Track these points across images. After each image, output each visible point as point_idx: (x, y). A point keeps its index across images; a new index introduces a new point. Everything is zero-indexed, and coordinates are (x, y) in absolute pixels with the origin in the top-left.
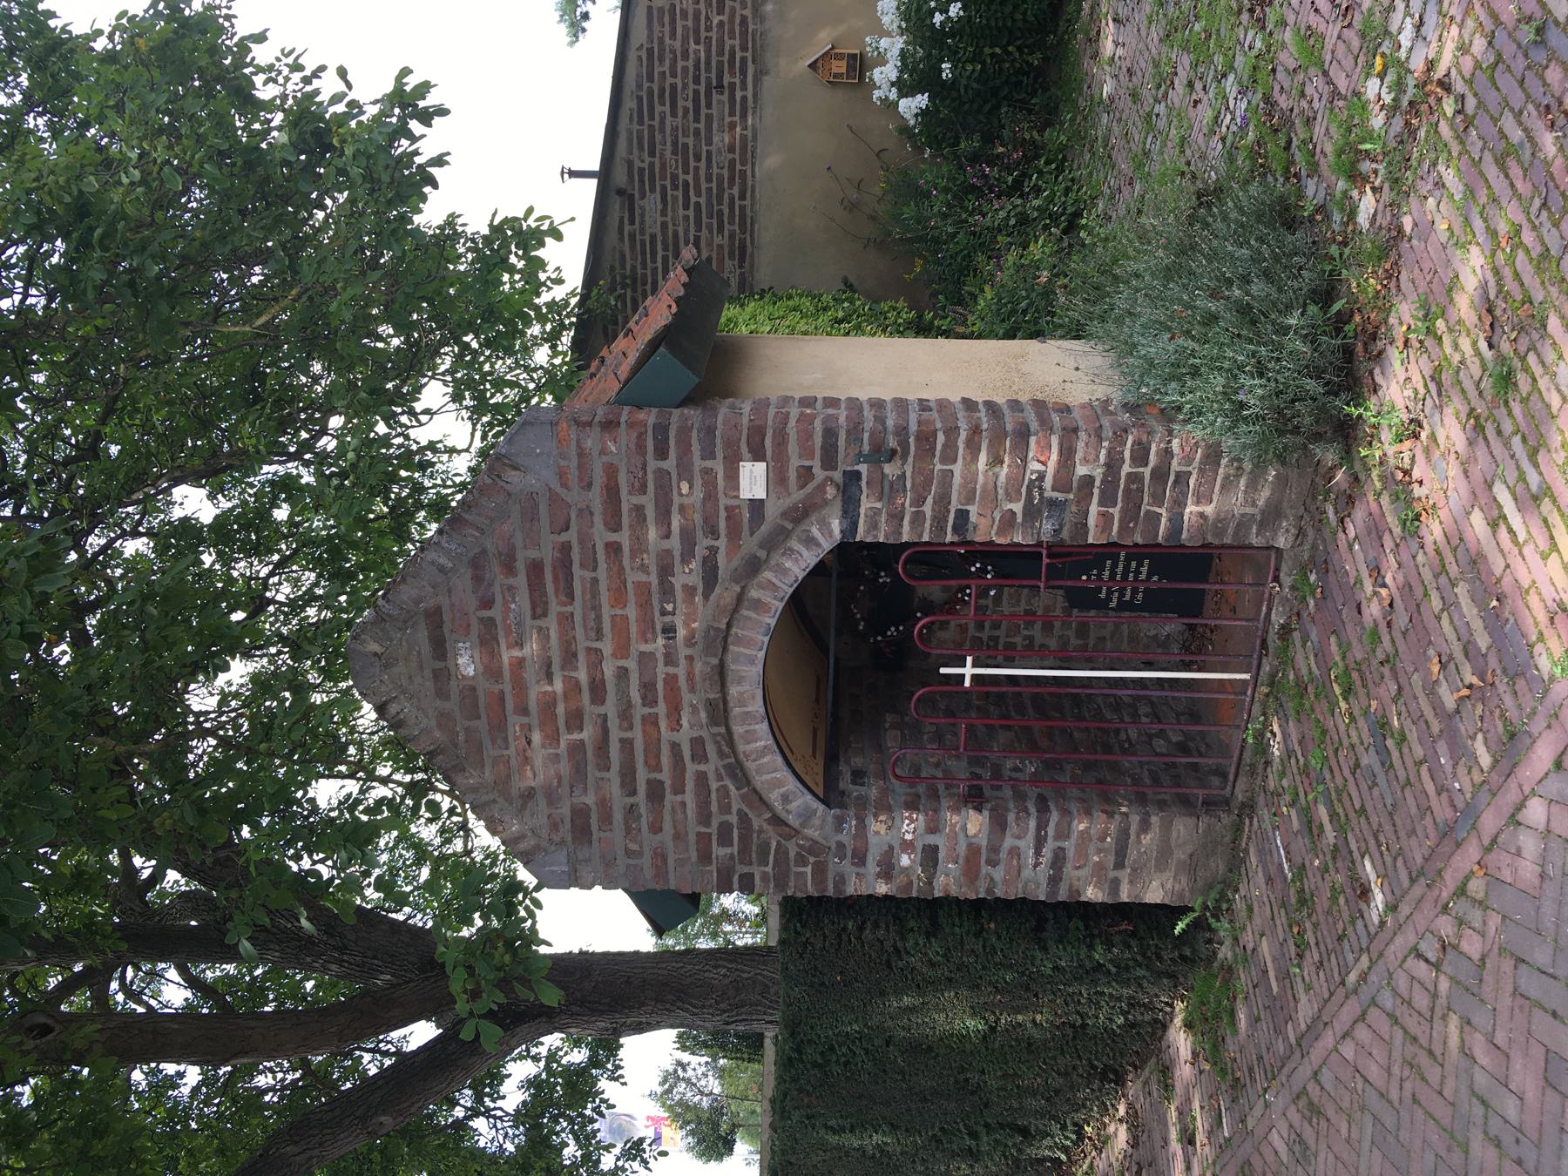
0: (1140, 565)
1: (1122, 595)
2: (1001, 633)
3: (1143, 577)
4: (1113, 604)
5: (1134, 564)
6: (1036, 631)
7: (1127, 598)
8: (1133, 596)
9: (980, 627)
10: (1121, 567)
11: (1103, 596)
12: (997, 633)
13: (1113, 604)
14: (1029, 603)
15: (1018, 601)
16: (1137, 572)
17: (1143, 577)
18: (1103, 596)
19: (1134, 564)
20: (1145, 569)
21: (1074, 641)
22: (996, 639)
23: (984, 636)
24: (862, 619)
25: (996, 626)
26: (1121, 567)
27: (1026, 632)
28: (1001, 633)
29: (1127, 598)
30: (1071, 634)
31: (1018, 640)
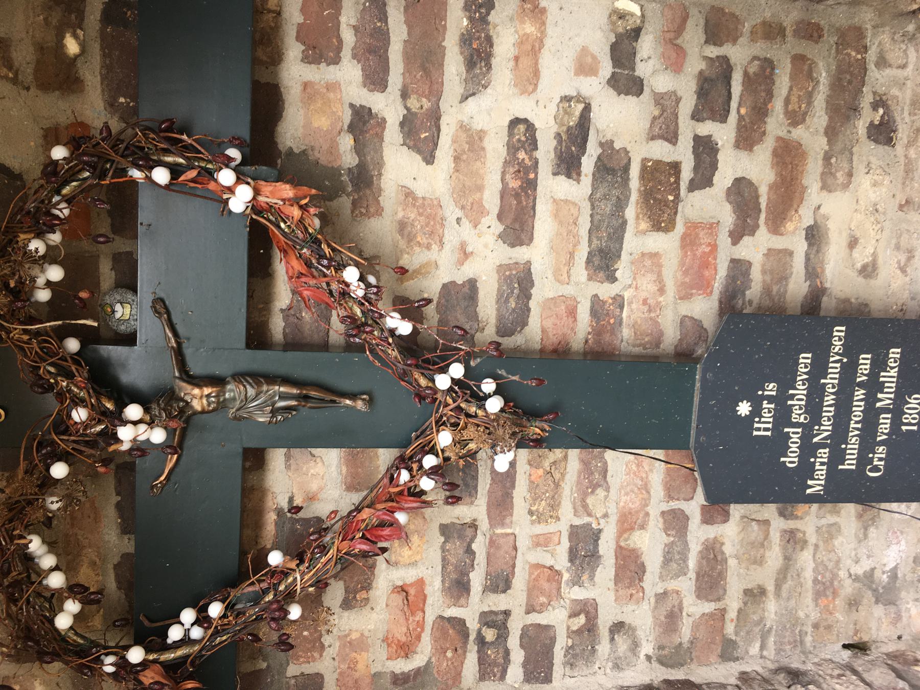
0: (879, 364)
1: (837, 456)
2: (513, 601)
3: (885, 399)
4: (816, 486)
5: (865, 362)
6: (601, 588)
7: (850, 464)
8: (863, 460)
9: (459, 587)
10: (834, 369)
11: (791, 460)
12: (499, 602)
13: (816, 486)
14: (582, 507)
15: (554, 506)
16: (874, 386)
17: (885, 399)
18: (791, 460)
19: (865, 362)
20: (890, 377)
21: (695, 608)
22: (497, 621)
23: (470, 613)
24: (74, 590)
25: (500, 583)
26: (834, 369)
27: (578, 593)
28: (513, 601)
29: (850, 464)
30: (686, 585)
31: (556, 617)
